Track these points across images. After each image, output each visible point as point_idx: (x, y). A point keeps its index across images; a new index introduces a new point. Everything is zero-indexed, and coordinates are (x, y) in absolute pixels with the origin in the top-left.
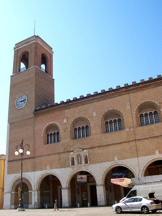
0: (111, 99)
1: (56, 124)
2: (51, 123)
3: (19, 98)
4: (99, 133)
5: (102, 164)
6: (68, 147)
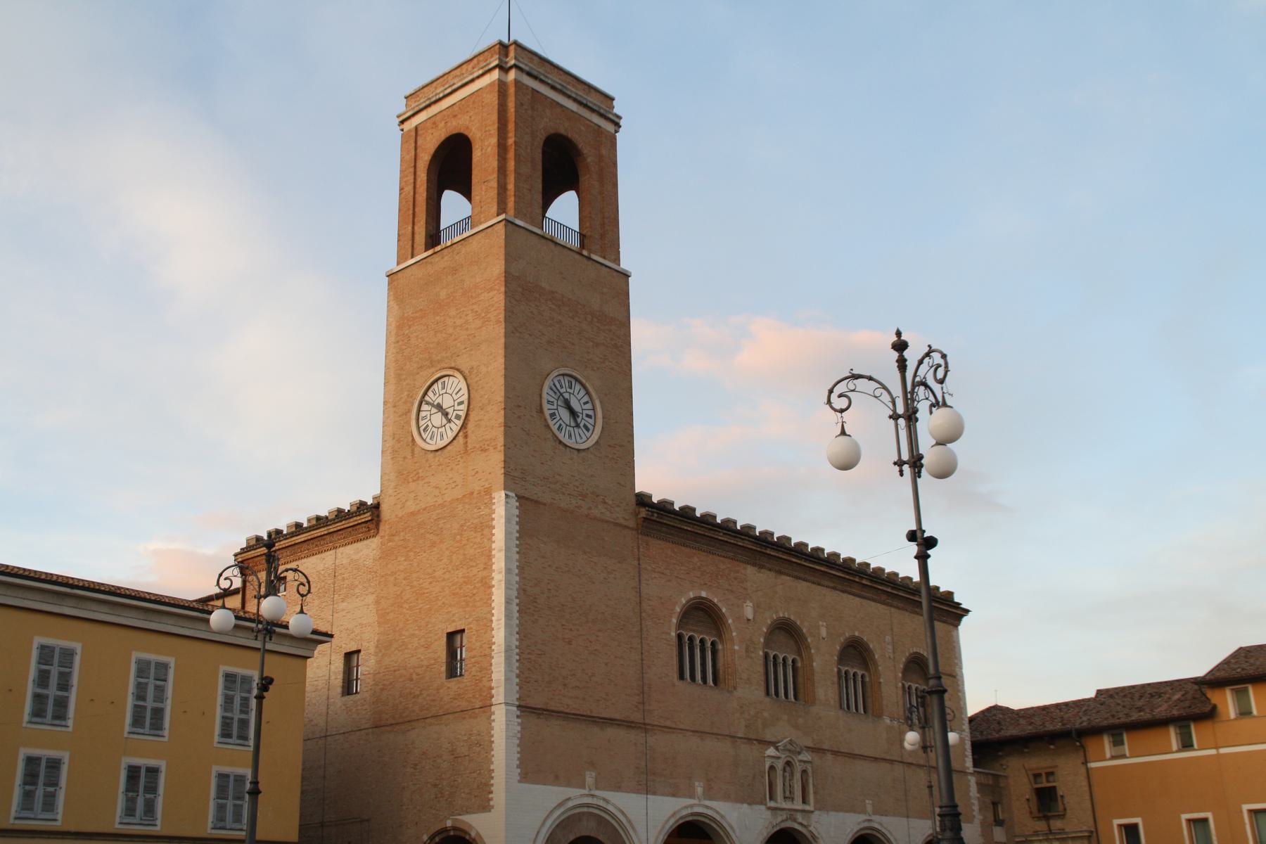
2: (704, 594)
3: (586, 399)
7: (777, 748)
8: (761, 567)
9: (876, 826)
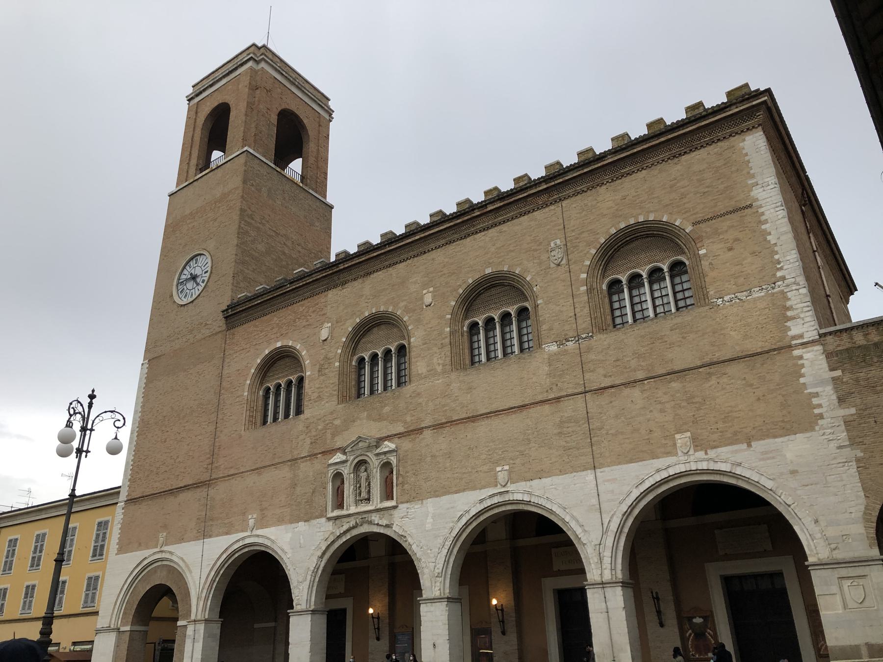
0: (490, 231)
1: (295, 349)
2: (279, 344)
4: (439, 369)
5: (445, 499)
6: (329, 436)
7: (345, 453)
8: (344, 283)
9: (519, 497)
